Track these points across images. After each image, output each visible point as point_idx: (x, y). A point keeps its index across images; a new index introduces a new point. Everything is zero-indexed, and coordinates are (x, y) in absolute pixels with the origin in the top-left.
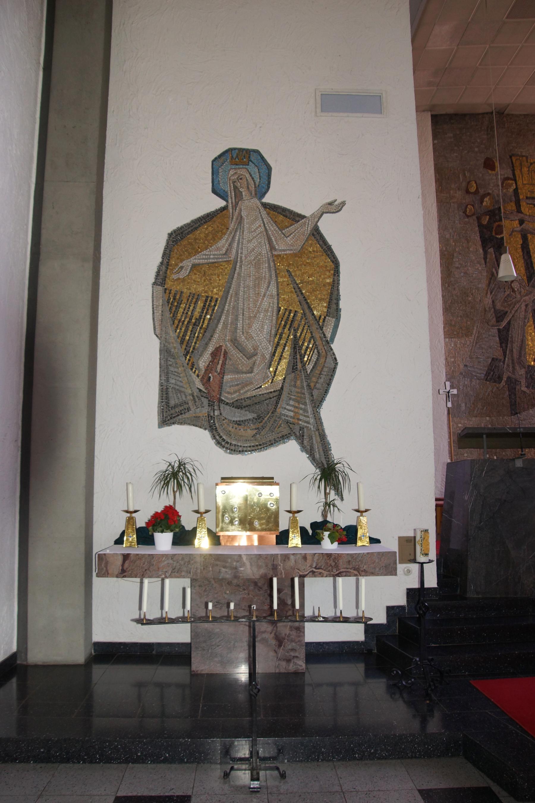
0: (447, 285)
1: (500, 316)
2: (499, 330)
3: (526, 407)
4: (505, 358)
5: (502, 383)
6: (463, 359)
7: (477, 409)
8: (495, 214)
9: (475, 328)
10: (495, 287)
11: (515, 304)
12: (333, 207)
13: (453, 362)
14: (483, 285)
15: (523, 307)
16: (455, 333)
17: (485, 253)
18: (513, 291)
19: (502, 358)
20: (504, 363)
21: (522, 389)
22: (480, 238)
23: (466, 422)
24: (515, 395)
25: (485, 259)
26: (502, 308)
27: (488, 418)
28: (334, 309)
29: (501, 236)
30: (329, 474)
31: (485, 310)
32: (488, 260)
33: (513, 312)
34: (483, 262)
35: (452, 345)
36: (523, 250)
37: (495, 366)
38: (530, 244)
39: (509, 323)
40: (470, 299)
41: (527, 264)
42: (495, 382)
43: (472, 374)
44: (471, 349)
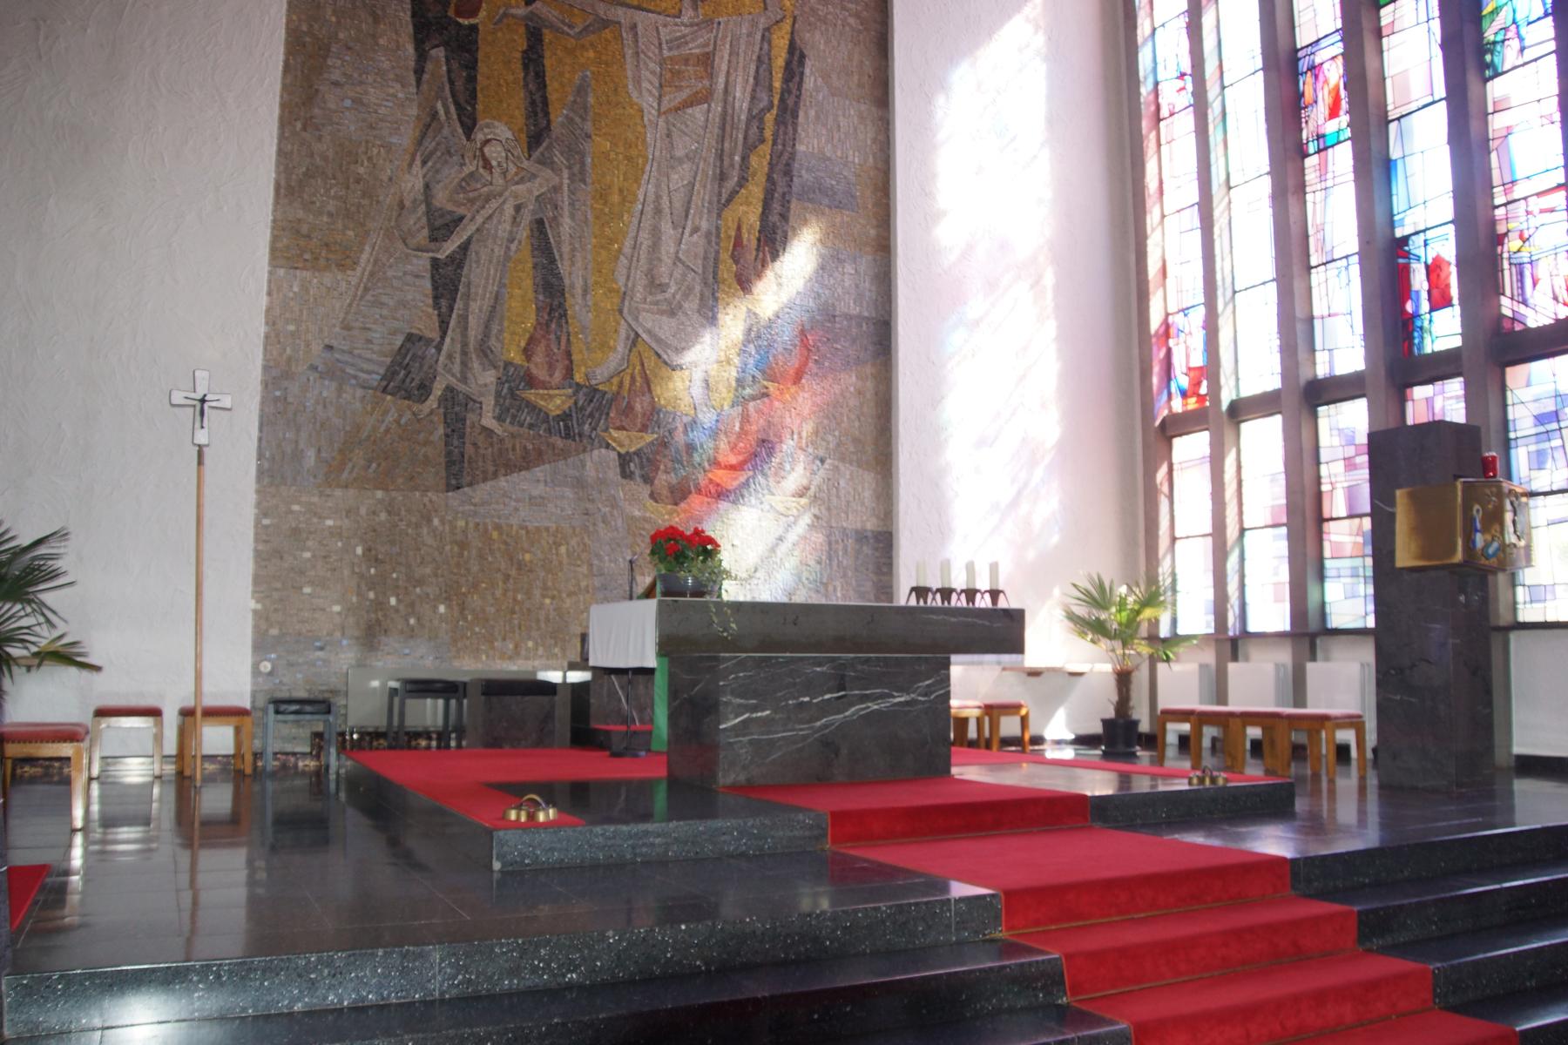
0: (299, 125)
1: (442, 226)
2: (435, 263)
3: (491, 469)
4: (443, 338)
5: (428, 402)
6: (321, 330)
7: (350, 465)
9: (367, 248)
10: (436, 150)
11: (487, 200)
13: (292, 334)
14: (405, 138)
15: (509, 210)
16: (307, 256)
17: (422, 56)
18: (487, 165)
19: (436, 336)
20: (439, 348)
21: (484, 422)
22: (414, 15)
23: (315, 499)
24: (462, 436)
25: (419, 72)
26: (449, 207)
27: (379, 494)
29: (473, 21)
31: (402, 206)
32: (426, 77)
33: (479, 219)
34: (412, 79)
35: (296, 289)
36: (526, 67)
37: (414, 357)
38: (547, 54)
39: (465, 248)
40: (361, 170)
41: (533, 103)
42: (408, 398)
43: (343, 371)
44: (350, 305)
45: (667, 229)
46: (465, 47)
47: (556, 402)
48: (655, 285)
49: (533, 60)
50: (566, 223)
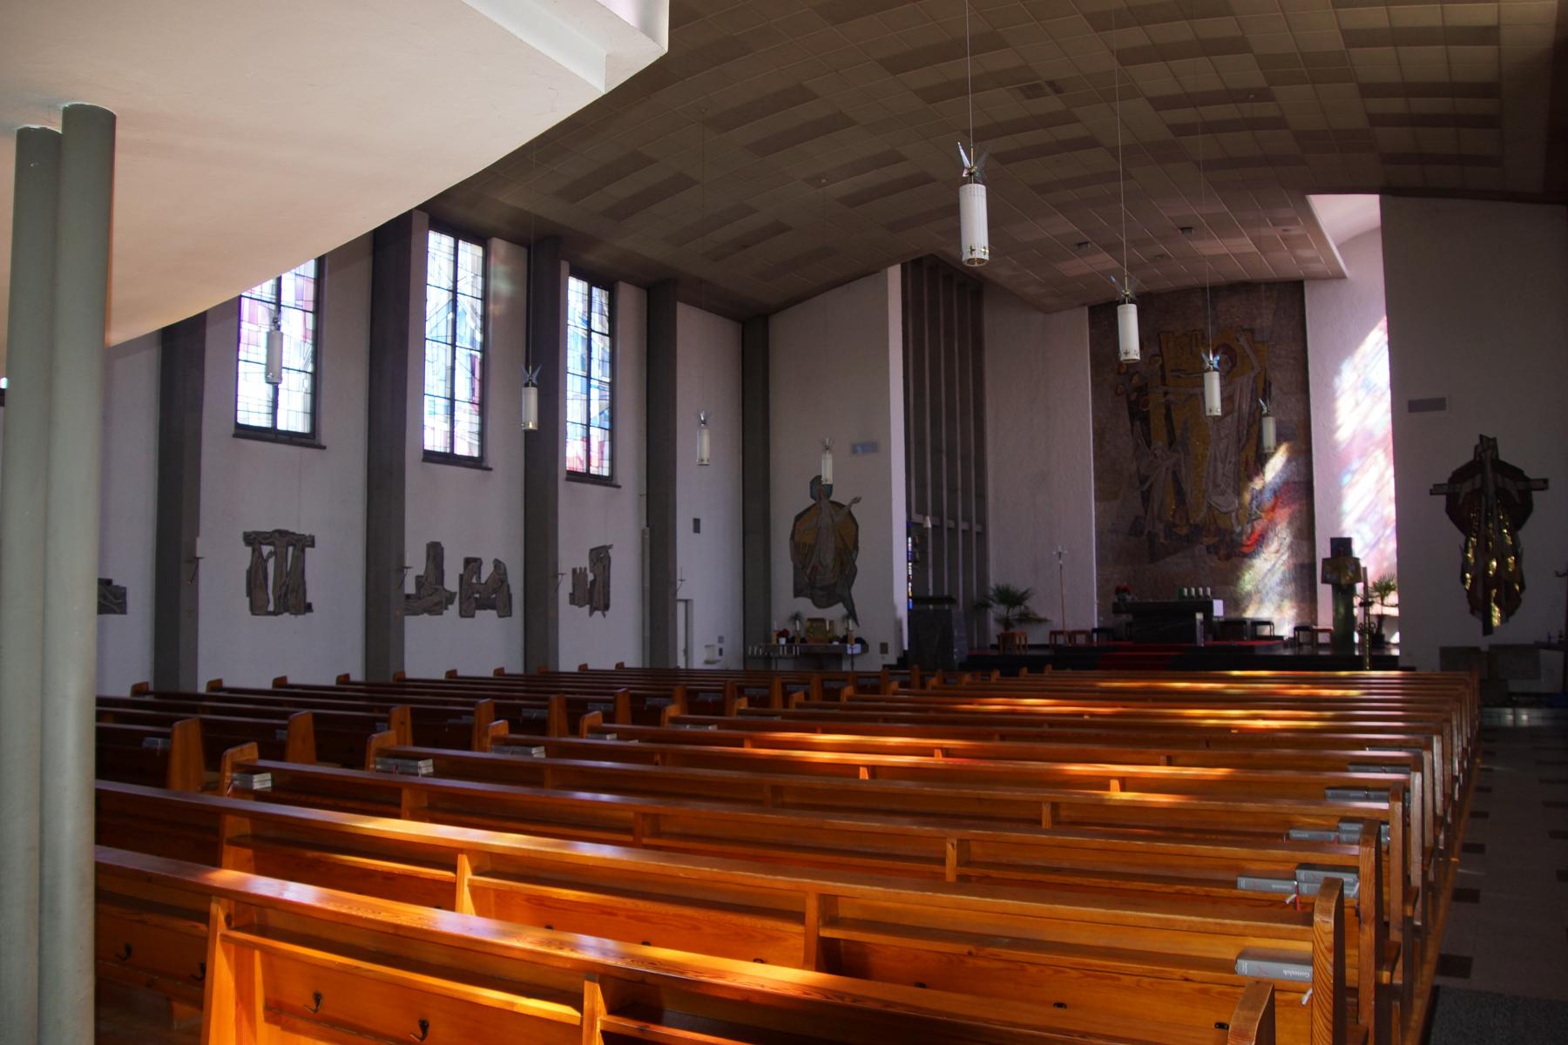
1: (1143, 480)
8: (1142, 390)
12: (856, 500)
28: (856, 547)
30: (852, 614)
45: (1220, 465)
46: (1145, 419)
47: (1184, 531)
48: (1216, 485)
49: (1168, 417)
50: (1184, 471)
